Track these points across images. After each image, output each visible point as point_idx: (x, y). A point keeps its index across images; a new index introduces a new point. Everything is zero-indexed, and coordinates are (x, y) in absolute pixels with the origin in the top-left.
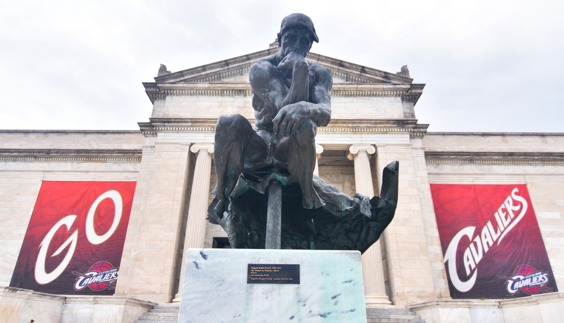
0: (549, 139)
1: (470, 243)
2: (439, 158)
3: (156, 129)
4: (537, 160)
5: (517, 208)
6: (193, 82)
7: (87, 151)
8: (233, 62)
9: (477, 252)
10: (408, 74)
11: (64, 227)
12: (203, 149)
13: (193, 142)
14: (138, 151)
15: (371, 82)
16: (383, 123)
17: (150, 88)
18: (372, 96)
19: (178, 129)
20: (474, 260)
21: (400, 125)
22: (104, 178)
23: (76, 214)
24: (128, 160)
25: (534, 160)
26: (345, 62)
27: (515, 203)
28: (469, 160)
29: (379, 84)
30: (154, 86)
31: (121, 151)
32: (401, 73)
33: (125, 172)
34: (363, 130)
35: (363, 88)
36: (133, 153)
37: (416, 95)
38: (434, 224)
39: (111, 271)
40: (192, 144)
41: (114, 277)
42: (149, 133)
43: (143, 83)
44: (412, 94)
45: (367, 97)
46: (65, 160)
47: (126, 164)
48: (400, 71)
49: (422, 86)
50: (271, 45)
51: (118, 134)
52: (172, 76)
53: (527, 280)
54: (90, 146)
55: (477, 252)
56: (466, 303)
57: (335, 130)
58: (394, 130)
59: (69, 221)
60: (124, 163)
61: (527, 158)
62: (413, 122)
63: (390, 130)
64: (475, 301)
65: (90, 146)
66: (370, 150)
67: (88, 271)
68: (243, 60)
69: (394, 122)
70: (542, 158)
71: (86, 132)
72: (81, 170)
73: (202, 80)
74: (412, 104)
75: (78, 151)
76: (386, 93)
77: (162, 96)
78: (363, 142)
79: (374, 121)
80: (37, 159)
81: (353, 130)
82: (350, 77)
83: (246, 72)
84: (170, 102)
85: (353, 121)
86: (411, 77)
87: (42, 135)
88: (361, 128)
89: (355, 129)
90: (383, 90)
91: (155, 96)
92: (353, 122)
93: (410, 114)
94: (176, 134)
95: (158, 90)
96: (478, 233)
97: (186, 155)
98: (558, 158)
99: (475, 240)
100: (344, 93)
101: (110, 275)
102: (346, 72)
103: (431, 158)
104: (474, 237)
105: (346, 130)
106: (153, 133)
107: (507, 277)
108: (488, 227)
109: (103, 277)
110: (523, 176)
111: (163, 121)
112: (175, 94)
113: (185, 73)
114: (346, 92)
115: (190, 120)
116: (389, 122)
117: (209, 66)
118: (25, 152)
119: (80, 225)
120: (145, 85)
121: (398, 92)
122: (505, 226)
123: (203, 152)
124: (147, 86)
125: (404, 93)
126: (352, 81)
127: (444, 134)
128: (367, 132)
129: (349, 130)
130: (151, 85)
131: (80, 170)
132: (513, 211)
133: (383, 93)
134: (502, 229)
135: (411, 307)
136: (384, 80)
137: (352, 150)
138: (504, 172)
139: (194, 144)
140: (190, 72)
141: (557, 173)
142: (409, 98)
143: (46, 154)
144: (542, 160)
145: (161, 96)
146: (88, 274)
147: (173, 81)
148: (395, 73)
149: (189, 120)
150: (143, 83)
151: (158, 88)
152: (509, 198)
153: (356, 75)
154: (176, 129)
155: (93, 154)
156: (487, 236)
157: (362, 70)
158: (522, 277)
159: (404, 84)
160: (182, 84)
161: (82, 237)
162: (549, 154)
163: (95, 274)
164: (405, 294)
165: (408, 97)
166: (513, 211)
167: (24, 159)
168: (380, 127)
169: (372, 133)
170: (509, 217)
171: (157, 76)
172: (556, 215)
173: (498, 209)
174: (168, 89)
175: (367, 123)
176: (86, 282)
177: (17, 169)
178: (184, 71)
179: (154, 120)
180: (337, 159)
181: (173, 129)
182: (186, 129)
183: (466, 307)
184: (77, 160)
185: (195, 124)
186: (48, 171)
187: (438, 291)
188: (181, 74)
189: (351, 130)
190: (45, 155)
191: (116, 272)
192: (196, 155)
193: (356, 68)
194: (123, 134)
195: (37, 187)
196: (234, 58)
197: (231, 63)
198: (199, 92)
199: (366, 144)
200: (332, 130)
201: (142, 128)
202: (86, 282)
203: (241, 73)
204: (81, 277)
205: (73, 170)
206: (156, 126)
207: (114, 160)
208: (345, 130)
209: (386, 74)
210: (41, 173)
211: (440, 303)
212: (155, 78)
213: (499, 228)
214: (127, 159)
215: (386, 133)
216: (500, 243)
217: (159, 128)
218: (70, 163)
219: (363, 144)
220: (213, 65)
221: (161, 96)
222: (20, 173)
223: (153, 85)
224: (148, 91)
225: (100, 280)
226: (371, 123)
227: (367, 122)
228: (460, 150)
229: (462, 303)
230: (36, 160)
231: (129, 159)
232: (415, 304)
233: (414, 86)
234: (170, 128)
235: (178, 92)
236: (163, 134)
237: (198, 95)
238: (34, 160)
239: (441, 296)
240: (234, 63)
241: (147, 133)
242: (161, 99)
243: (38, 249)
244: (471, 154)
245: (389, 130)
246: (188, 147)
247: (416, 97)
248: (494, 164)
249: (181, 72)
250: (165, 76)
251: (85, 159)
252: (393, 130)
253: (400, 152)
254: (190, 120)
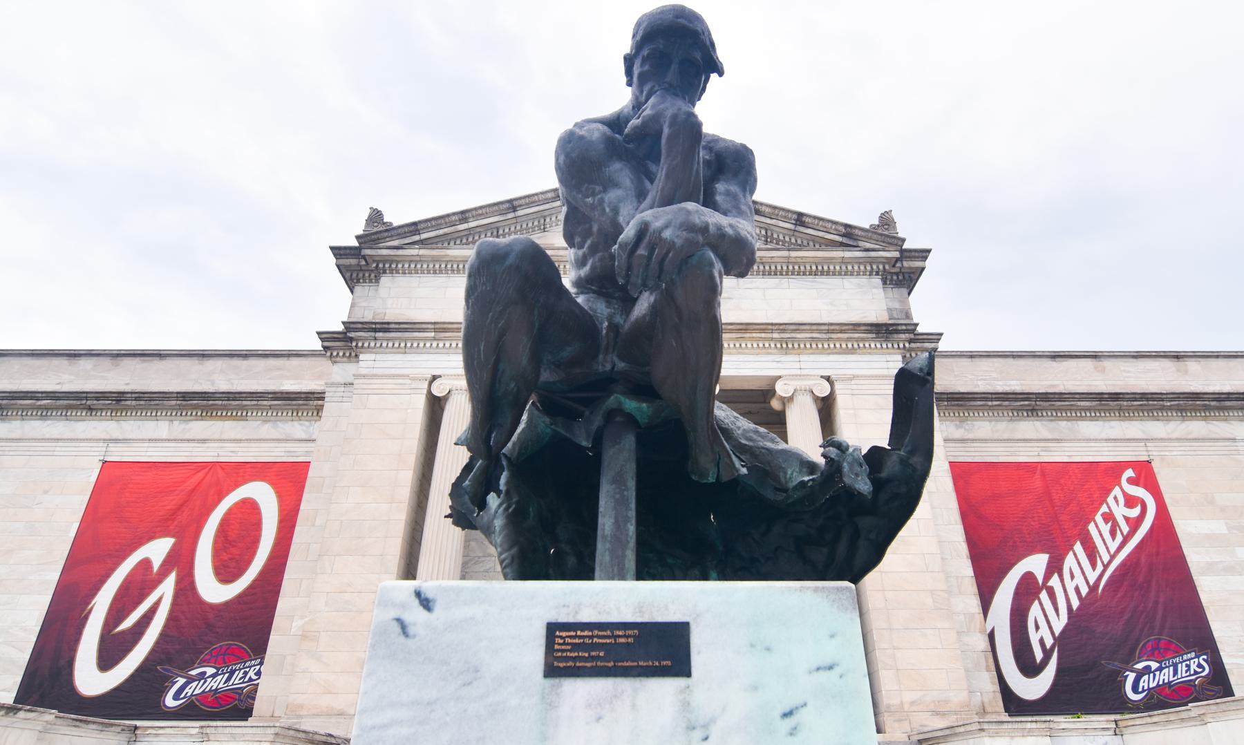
0: (1192, 365)
1: (1040, 590)
2: (966, 406)
3: (356, 346)
4: (1170, 408)
5: (1135, 512)
6: (440, 245)
7: (203, 395)
8: (527, 204)
9: (1057, 610)
10: (895, 227)
11: (146, 563)
12: (459, 388)
13: (436, 373)
14: (316, 396)
15: (817, 246)
16: (844, 330)
17: (347, 258)
18: (819, 273)
19: (406, 344)
20: (1050, 627)
21: (880, 335)
22: (240, 454)
23: (173, 537)
24: (295, 414)
25: (1162, 408)
26: (762, 204)
27: (1130, 501)
28: (1027, 410)
29: (835, 249)
30: (354, 255)
31: (279, 395)
32: (878, 226)
33: (286, 440)
34: (802, 346)
35: (802, 258)
36: (307, 399)
37: (913, 273)
38: (963, 548)
39: (247, 664)
40: (434, 378)
41: (254, 677)
42: (341, 354)
43: (332, 248)
44: (903, 270)
45: (811, 277)
46: (156, 416)
47: (290, 423)
49: (924, 254)
51: (276, 359)
52: (393, 233)
53: (1166, 671)
54: (213, 384)
55: (1057, 610)
56: (1043, 726)
57: (743, 345)
58: (870, 345)
59: (157, 550)
60: (286, 421)
61: (1149, 405)
62: (909, 328)
63: (861, 345)
64: (1062, 721)
65: (213, 384)
66: (820, 388)
67: (196, 665)
68: (546, 199)
69: (869, 328)
70: (1178, 405)
71: (203, 355)
72: (191, 437)
73: (458, 242)
74: (905, 291)
75: (185, 396)
76: (850, 268)
77: (373, 275)
78: (804, 372)
79: (826, 327)
80: (94, 414)
81: (781, 345)
82: (772, 234)
83: (554, 224)
84: (390, 288)
85: (781, 327)
86: (900, 235)
87: (107, 362)
88: (799, 341)
89: (787, 345)
90: (844, 261)
91: (357, 275)
92: (782, 330)
93: (901, 311)
94: (399, 357)
95: (363, 263)
96: (1055, 567)
97: (420, 402)
98: (1213, 403)
99: (1050, 584)
100: (761, 267)
101: (246, 673)
102: (765, 226)
103: (948, 405)
104: (1047, 577)
105: (767, 345)
106: (350, 354)
107: (1123, 666)
108: (1075, 554)
109: (228, 679)
110: (1143, 444)
111: (373, 328)
112: (400, 272)
113: (422, 226)
114: (764, 267)
115: (432, 326)
116: (856, 328)
117: (474, 213)
118: (68, 398)
119: (181, 561)
120: (337, 251)
121: (875, 267)
122: (1112, 552)
123: (459, 394)
124: (341, 255)
125: (887, 267)
126: (777, 244)
127: (972, 356)
128: (811, 351)
129: (773, 345)
130: (348, 251)
131: (187, 436)
132: (1127, 519)
133: (844, 268)
134: (1106, 558)
135: (921, 737)
136: (845, 240)
137: (781, 389)
138: (1104, 436)
139: (440, 376)
140: (434, 224)
141: (1214, 436)
142: (898, 278)
143: (114, 402)
144: (1180, 409)
145: (370, 276)
146: (194, 672)
147: (396, 243)
148: (867, 226)
149: (430, 326)
150: (332, 248)
151: (364, 257)
152: (1117, 491)
153: (785, 232)
154: (400, 344)
155: (217, 402)
156: (1075, 574)
157: (797, 220)
158: (1154, 665)
159: (887, 249)
160: (417, 249)
161: (186, 588)
162: (1195, 396)
163: (210, 671)
164: (906, 707)
165: (895, 278)
166: (1127, 519)
167: (64, 414)
168: (839, 339)
169: (823, 351)
170: (1118, 532)
171: (362, 232)
172: (1218, 527)
173: (1095, 516)
174: (385, 260)
175: (812, 331)
176: (189, 691)
177: (47, 436)
178: (420, 222)
179: (352, 326)
180: (747, 410)
181: (394, 344)
182: (421, 345)
183: (1045, 734)
184: (181, 415)
185: (443, 335)
186: (116, 441)
187: (977, 699)
188: (415, 227)
189: (779, 346)
190: (109, 404)
191: (258, 667)
192: (442, 403)
193: (785, 217)
194: (286, 358)
195: (90, 476)
196: (528, 196)
197: (520, 206)
198: (452, 266)
199: (811, 375)
200: (738, 345)
201: (326, 344)
202: (189, 691)
203: (542, 227)
204: (179, 678)
205: (172, 438)
206: (357, 340)
207: (264, 414)
208: (764, 345)
209: (849, 229)
210: (101, 444)
211: (985, 726)
212: (358, 237)
213: (1100, 557)
214: (293, 413)
215: (852, 351)
216: (1103, 589)
217: (363, 344)
218: (167, 423)
219: (804, 375)
220: (484, 210)
221: (370, 276)
222: (54, 444)
223: (352, 252)
224: (341, 265)
225: (221, 686)
226: (820, 331)
227: (810, 330)
228: (1007, 389)
229: (1034, 725)
230: (91, 415)
231: (298, 413)
232: (930, 729)
233: (908, 254)
234: (388, 344)
235: (406, 266)
236: (372, 356)
237: (450, 272)
238: (86, 415)
239: (983, 711)
240: (529, 205)
241: (338, 354)
242: (371, 281)
243: (83, 615)
244: (1031, 396)
245: (858, 345)
246: (425, 385)
247: (912, 275)
248: (1081, 418)
249: (415, 224)
250: (381, 232)
251: (199, 414)
252: (867, 345)
253: (883, 392)
254: (432, 326)
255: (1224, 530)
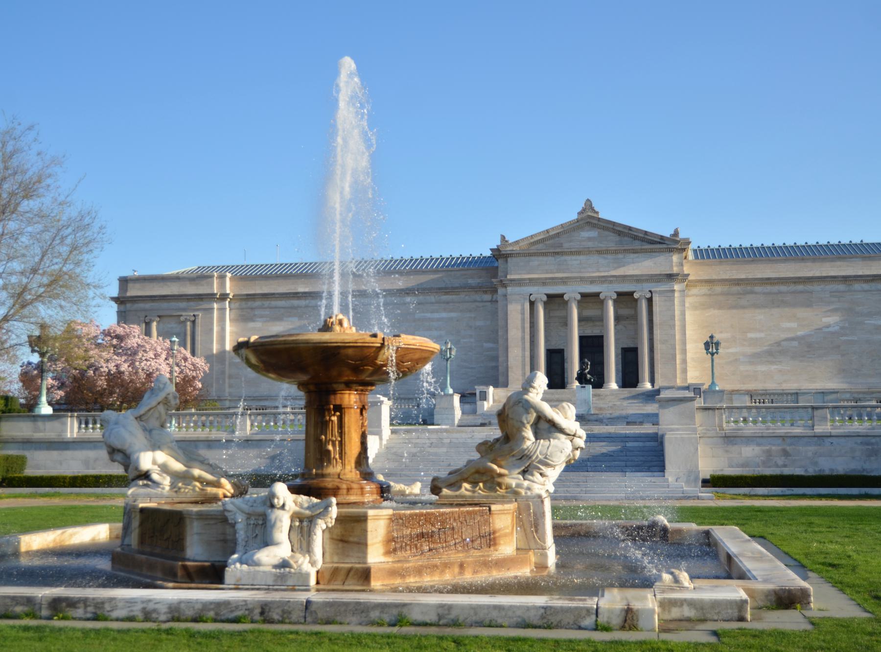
13: (531, 293)
48: (673, 233)
50: (579, 213)
172: (794, 325)
174: (508, 254)
236: (510, 288)
255: (796, 326)
